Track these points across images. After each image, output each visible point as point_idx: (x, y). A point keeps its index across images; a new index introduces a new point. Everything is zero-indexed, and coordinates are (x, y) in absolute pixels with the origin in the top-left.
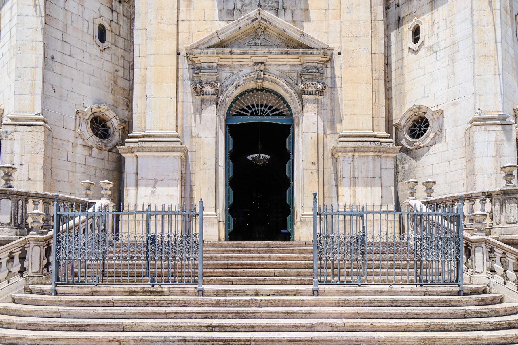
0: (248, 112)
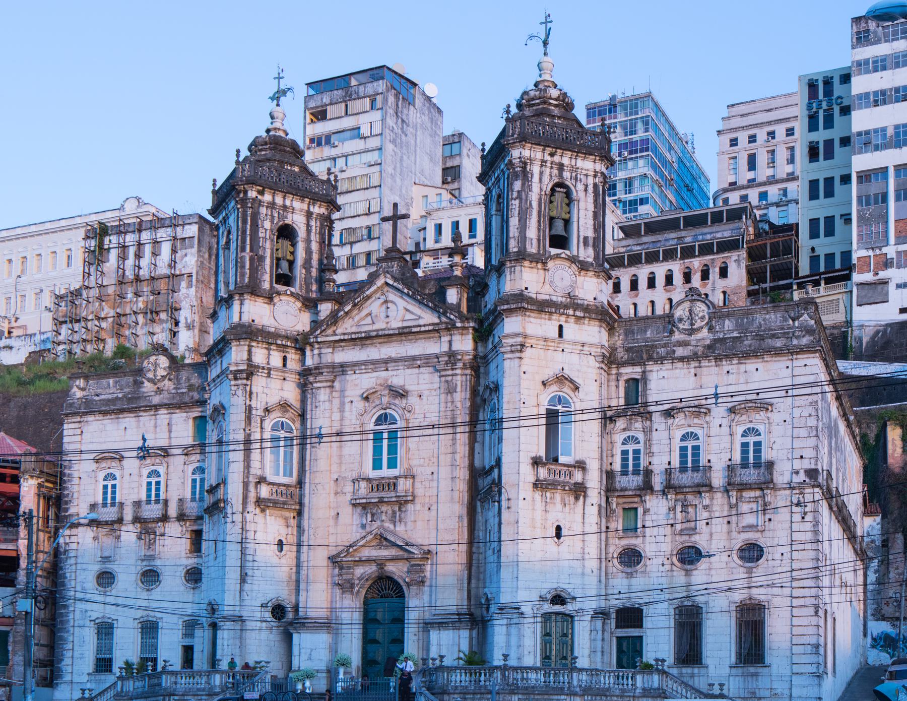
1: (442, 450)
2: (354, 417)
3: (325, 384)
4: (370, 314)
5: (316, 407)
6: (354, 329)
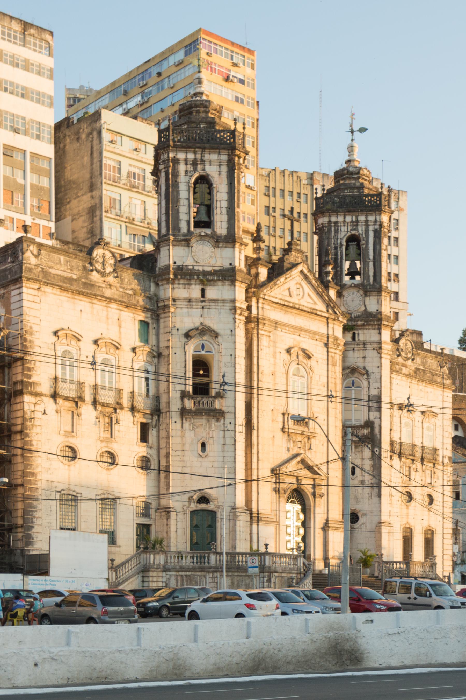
6: (280, 297)
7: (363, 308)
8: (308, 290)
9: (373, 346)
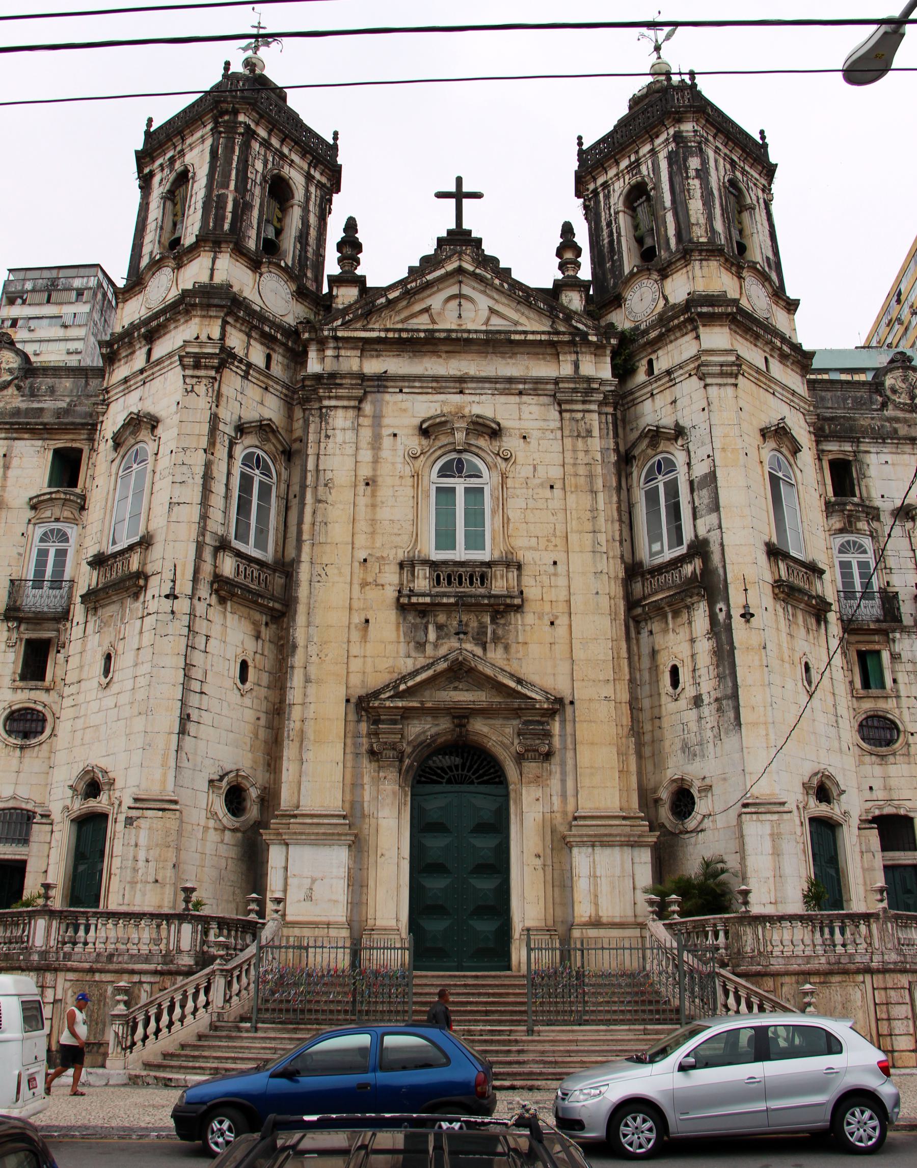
0: (443, 778)
1: (574, 525)
2: (400, 459)
3: (345, 403)
4: (427, 310)
5: (328, 437)
7: (662, 303)
8: (491, 303)
9: (686, 369)
